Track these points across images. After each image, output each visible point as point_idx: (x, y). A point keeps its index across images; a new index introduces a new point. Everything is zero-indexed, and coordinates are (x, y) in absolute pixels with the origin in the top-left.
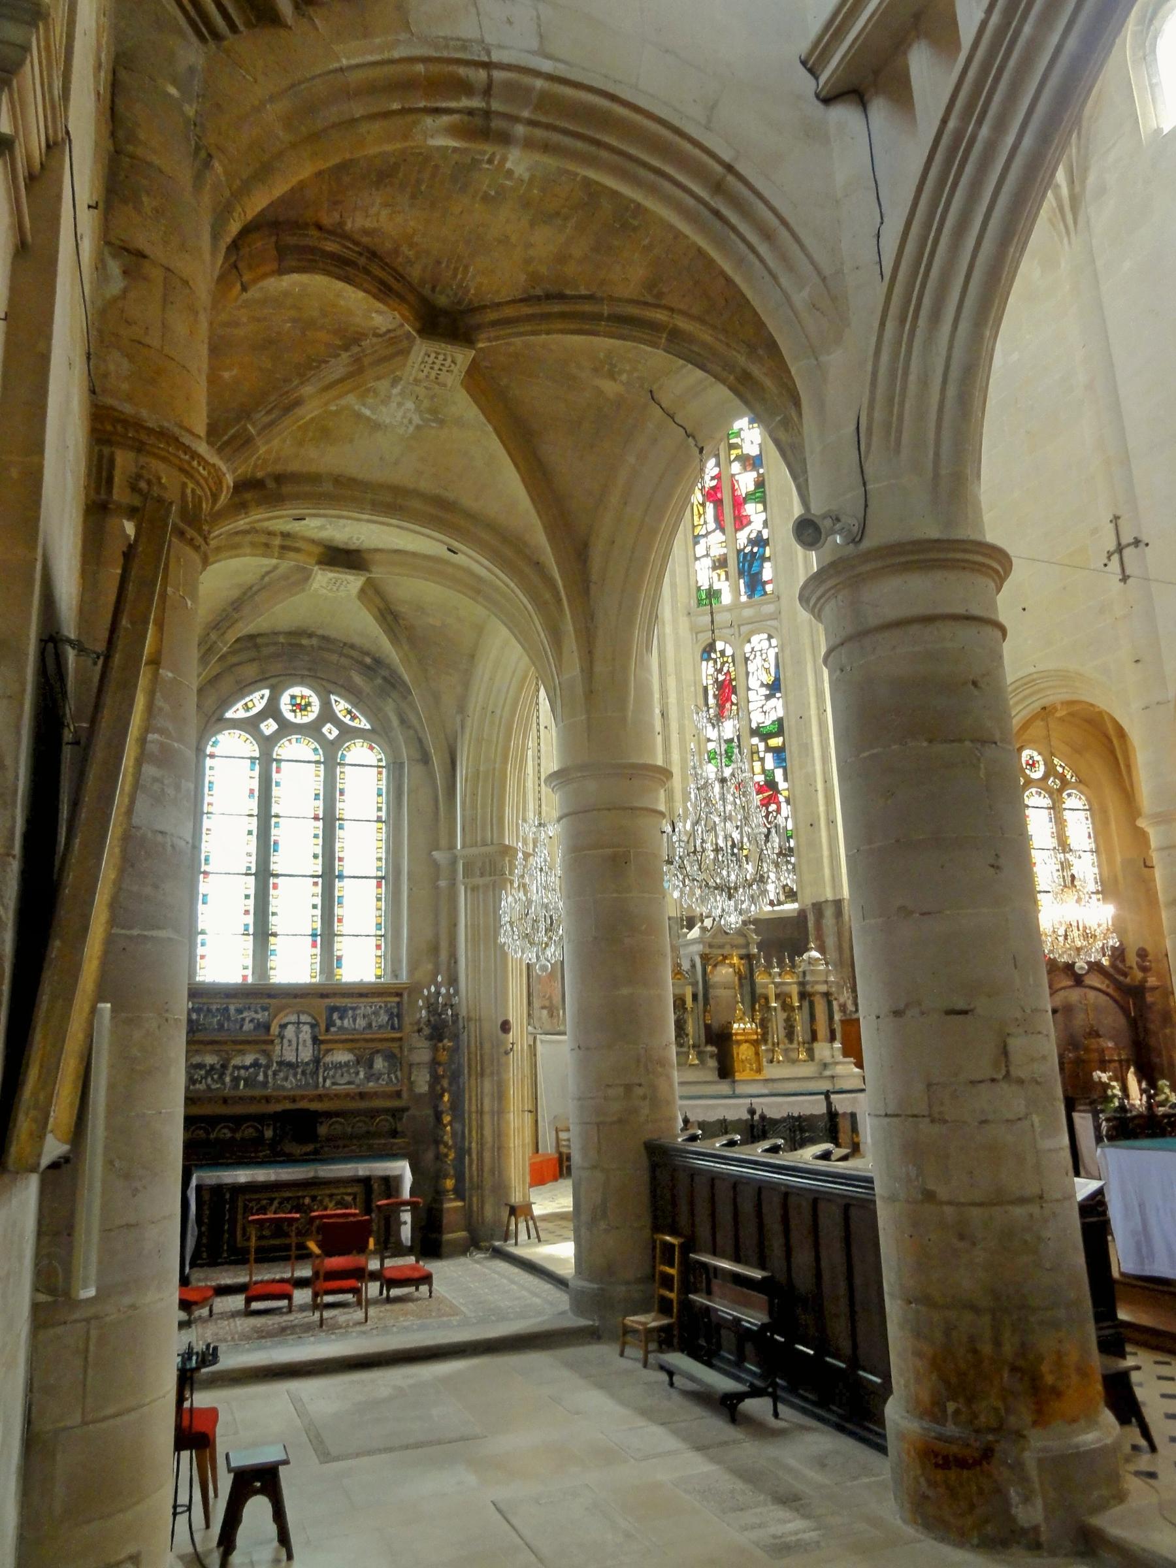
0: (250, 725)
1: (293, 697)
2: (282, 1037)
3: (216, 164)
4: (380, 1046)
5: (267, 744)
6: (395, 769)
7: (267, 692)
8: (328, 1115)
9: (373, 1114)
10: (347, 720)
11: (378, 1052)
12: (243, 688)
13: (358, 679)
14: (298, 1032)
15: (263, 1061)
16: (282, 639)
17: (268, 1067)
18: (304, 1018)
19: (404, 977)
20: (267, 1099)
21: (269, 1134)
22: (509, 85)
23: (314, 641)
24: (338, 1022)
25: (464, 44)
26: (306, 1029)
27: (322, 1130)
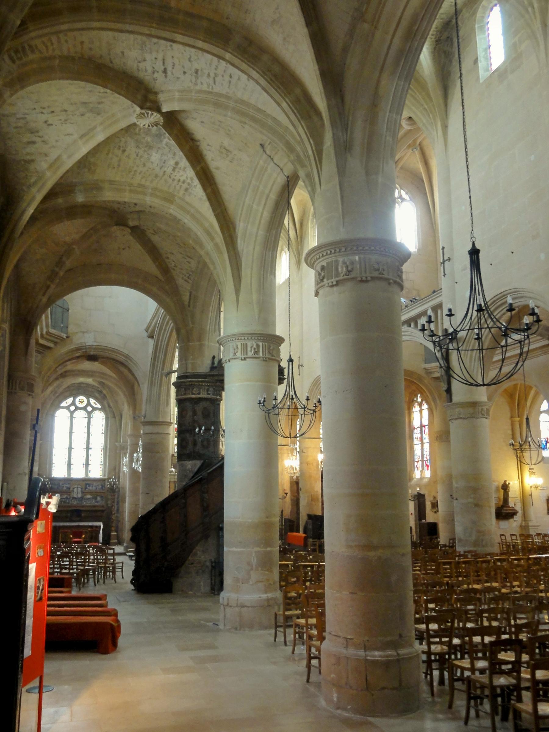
0: (68, 408)
1: (79, 399)
2: (73, 491)
3: (43, 373)
4: (98, 494)
5: (72, 413)
6: (107, 419)
7: (72, 398)
8: (85, 511)
9: (96, 511)
10: (94, 405)
11: (98, 495)
12: (66, 398)
13: (97, 395)
14: (78, 490)
15: (68, 497)
16: (76, 385)
17: (69, 498)
18: (79, 486)
19: (106, 477)
20: (69, 507)
21: (69, 515)
22: (89, 348)
23: (85, 385)
24: (88, 488)
25: (81, 343)
26: (80, 489)
27: (83, 515)
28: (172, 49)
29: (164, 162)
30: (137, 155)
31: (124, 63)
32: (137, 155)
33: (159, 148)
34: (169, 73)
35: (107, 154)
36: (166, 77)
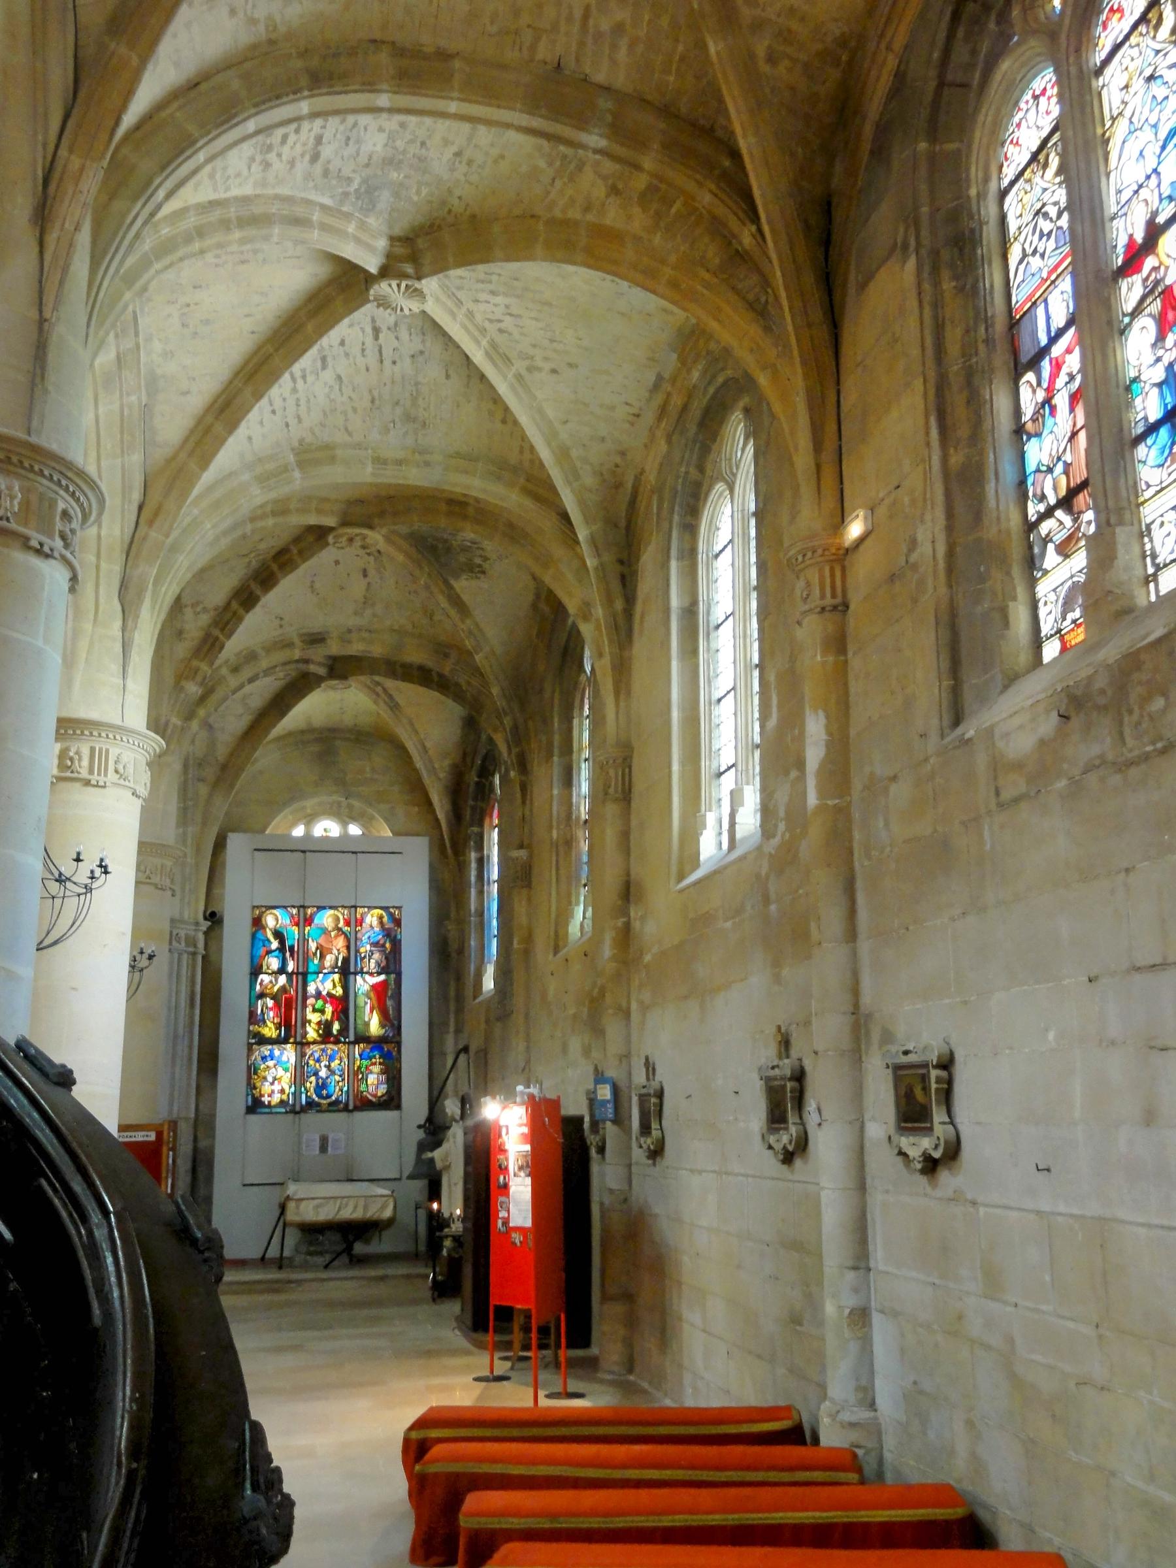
28: (370, 391)
29: (348, 139)
30: (423, 144)
31: (446, 350)
32: (423, 144)
33: (367, 165)
34: (369, 330)
35: (502, 157)
36: (373, 320)
